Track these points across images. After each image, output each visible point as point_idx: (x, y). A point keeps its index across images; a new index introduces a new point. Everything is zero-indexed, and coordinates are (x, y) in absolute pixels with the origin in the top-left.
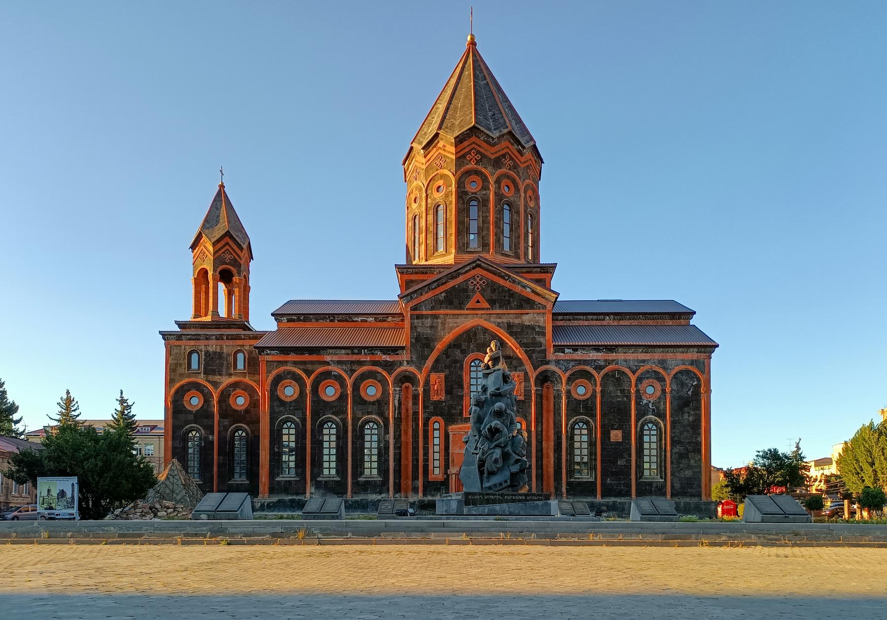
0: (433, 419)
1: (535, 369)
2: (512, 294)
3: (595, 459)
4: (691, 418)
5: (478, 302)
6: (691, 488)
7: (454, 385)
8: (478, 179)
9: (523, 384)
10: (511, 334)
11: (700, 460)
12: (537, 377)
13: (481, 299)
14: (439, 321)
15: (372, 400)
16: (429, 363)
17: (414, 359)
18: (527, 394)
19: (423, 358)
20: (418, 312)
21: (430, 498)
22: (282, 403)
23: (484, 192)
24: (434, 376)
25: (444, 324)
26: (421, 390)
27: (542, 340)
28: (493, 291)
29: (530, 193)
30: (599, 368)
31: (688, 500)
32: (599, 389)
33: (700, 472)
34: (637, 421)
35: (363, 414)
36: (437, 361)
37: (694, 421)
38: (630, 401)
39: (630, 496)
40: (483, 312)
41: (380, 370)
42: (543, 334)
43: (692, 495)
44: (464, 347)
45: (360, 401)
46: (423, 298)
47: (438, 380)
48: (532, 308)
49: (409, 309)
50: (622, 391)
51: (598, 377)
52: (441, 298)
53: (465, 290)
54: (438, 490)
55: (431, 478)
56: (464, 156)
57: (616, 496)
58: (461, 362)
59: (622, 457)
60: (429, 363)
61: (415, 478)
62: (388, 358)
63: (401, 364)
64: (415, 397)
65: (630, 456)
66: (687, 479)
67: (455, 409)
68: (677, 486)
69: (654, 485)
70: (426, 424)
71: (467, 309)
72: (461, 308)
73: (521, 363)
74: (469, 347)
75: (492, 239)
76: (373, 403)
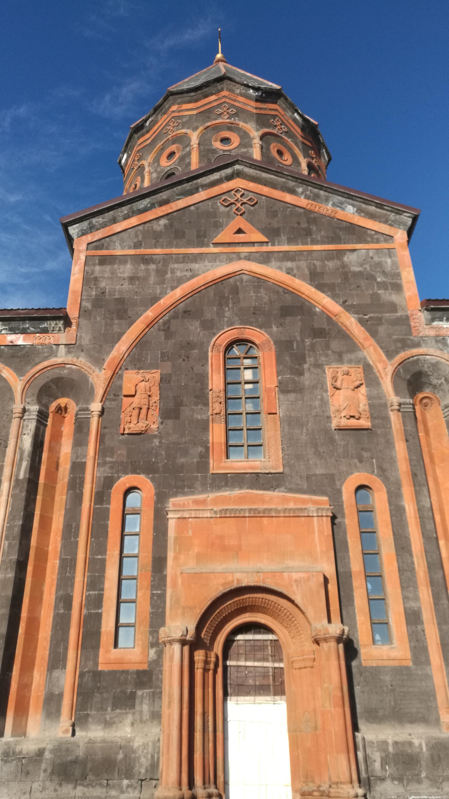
0: (125, 480)
1: (390, 355)
5: (240, 231)
7: (181, 398)
9: (363, 390)
10: (320, 287)
12: (396, 375)
14: (152, 267)
16: (122, 347)
17: (86, 339)
18: (378, 409)
20: (104, 252)
21: (95, 733)
23: (244, 150)
24: (131, 379)
25: (161, 273)
26: (96, 407)
27: (394, 298)
36: (141, 344)
42: (397, 287)
44: (208, 316)
46: (118, 227)
47: (141, 384)
49: (84, 246)
54: (126, 701)
55: (108, 658)
60: (122, 347)
61: (57, 661)
62: (20, 340)
63: (51, 351)
64: (81, 427)
67: (185, 453)
70: (102, 496)
72: (201, 244)
74: (220, 314)
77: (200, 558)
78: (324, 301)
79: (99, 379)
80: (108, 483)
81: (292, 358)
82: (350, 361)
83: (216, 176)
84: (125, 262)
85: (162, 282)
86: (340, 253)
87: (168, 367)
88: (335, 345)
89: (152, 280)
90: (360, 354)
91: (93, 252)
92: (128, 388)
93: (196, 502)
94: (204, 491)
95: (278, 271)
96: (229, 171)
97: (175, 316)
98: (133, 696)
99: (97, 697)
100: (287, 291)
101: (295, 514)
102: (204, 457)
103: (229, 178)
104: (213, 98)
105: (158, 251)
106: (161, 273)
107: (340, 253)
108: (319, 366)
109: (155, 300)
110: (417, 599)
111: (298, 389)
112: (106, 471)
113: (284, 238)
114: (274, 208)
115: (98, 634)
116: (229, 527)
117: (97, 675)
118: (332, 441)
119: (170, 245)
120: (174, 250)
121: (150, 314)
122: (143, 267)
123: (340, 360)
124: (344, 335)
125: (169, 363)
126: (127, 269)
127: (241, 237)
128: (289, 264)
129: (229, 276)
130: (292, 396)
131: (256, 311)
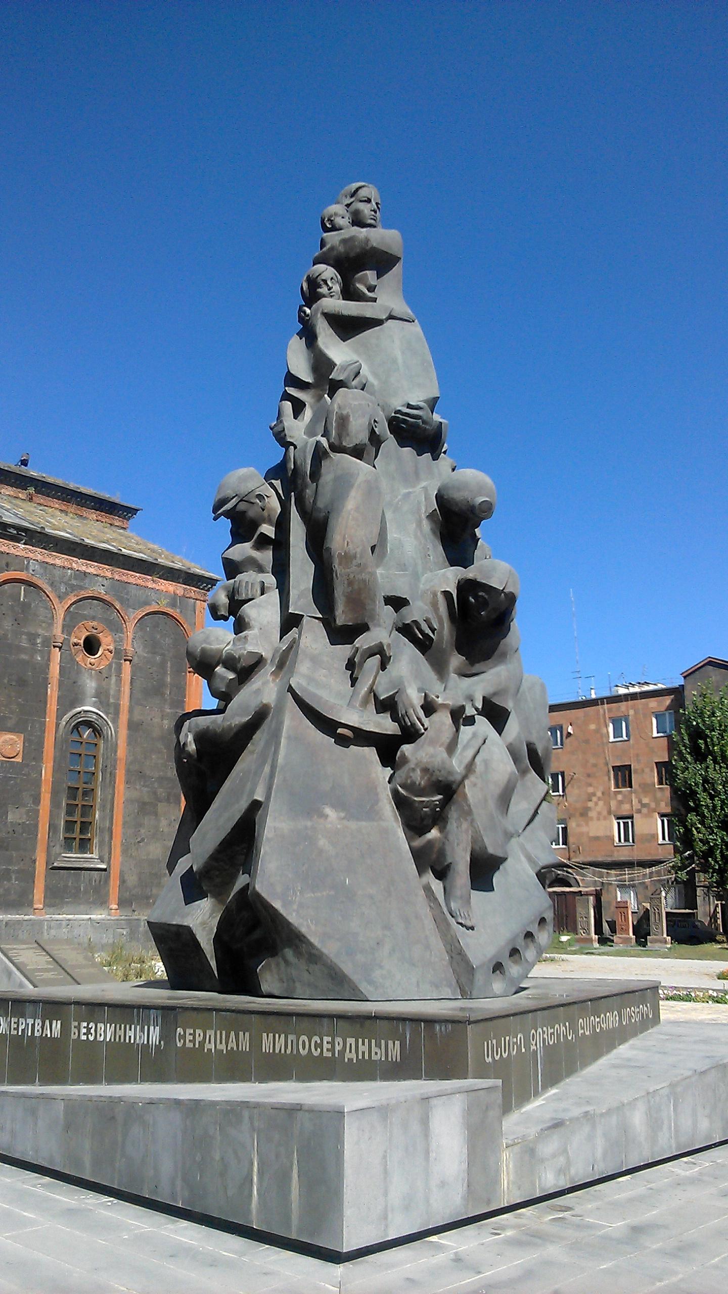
34: (59, 717)
39: (31, 904)
59: (19, 804)
65: (37, 800)
68: (132, 880)
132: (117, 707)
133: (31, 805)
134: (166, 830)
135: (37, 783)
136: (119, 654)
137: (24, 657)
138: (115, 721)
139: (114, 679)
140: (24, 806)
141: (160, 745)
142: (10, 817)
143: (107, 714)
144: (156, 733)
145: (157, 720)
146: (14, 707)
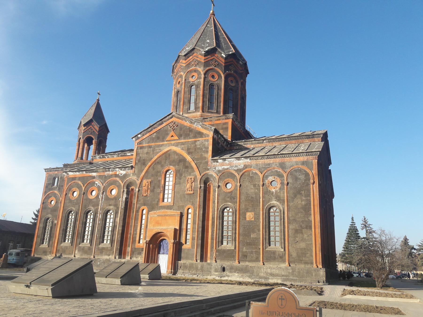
2: (191, 130)
3: (235, 233)
4: (303, 203)
5: (172, 136)
6: (305, 256)
8: (195, 74)
9: (193, 184)
10: (189, 153)
11: (311, 235)
13: (174, 134)
14: (152, 149)
15: (113, 197)
17: (136, 172)
19: (142, 171)
20: (141, 145)
22: (71, 201)
23: (199, 80)
25: (153, 151)
26: (137, 190)
27: (206, 155)
28: (181, 129)
29: (230, 79)
30: (238, 171)
31: (303, 266)
32: (239, 184)
33: (312, 244)
35: (107, 206)
37: (306, 205)
38: (260, 192)
39: (260, 261)
40: (175, 142)
41: (118, 179)
42: (207, 152)
43: (306, 263)
45: (107, 199)
46: (144, 137)
48: (201, 137)
50: (255, 185)
51: (238, 177)
52: (154, 136)
53: (166, 131)
56: (189, 64)
57: (249, 261)
58: (160, 172)
59: (254, 232)
60: (143, 173)
65: (259, 230)
66: (301, 249)
67: (154, 201)
68: (294, 254)
69: (277, 254)
71: (167, 141)
73: (193, 171)
74: (165, 163)
75: (200, 105)
76: (112, 199)
77: (154, 226)
78: (188, 158)
79: (138, 182)
80: (139, 208)
81: (178, 175)
82: (192, 175)
83: (168, 118)
84: (145, 148)
85: (153, 154)
86: (196, 141)
87: (152, 179)
88: (190, 170)
89: (151, 153)
90: (195, 173)
91: (138, 145)
92: (144, 185)
93: (154, 213)
94: (157, 210)
95: (180, 149)
96: (171, 116)
97: (155, 164)
98: (141, 253)
99: (135, 253)
100: (181, 155)
101: (174, 215)
102: (158, 201)
103: (172, 118)
104: (191, 57)
105: (153, 144)
106: (153, 151)
107: (196, 141)
108: (185, 177)
109: (152, 159)
110: (195, 235)
111: (180, 183)
112: (138, 206)
113: (183, 137)
114: (182, 127)
115: (135, 241)
116: (159, 219)
117: (135, 248)
118: (185, 197)
119: (156, 142)
120: (157, 144)
121: (149, 164)
122: (149, 149)
123: (190, 175)
124: (192, 168)
125: (153, 177)
126: (146, 150)
127: (172, 138)
128: (183, 146)
129: (168, 151)
130: (178, 185)
131: (174, 161)
132: (284, 201)
133: (257, 232)
134: (307, 238)
135: (259, 226)
136: (282, 183)
137: (252, 191)
138: (283, 204)
139: (282, 192)
140: (256, 232)
141: (302, 210)
142: (252, 236)
143: (280, 203)
144: (300, 206)
145: (300, 202)
146: (251, 205)
